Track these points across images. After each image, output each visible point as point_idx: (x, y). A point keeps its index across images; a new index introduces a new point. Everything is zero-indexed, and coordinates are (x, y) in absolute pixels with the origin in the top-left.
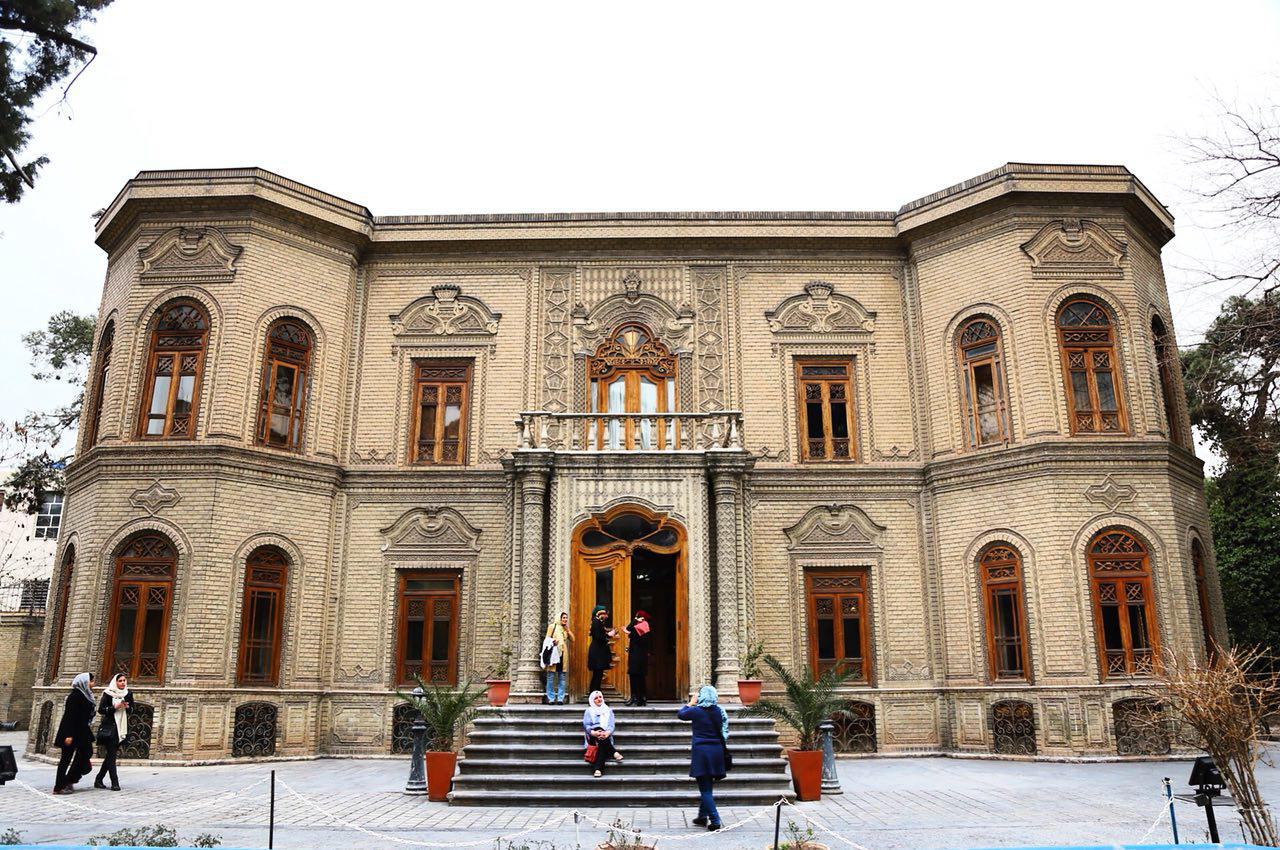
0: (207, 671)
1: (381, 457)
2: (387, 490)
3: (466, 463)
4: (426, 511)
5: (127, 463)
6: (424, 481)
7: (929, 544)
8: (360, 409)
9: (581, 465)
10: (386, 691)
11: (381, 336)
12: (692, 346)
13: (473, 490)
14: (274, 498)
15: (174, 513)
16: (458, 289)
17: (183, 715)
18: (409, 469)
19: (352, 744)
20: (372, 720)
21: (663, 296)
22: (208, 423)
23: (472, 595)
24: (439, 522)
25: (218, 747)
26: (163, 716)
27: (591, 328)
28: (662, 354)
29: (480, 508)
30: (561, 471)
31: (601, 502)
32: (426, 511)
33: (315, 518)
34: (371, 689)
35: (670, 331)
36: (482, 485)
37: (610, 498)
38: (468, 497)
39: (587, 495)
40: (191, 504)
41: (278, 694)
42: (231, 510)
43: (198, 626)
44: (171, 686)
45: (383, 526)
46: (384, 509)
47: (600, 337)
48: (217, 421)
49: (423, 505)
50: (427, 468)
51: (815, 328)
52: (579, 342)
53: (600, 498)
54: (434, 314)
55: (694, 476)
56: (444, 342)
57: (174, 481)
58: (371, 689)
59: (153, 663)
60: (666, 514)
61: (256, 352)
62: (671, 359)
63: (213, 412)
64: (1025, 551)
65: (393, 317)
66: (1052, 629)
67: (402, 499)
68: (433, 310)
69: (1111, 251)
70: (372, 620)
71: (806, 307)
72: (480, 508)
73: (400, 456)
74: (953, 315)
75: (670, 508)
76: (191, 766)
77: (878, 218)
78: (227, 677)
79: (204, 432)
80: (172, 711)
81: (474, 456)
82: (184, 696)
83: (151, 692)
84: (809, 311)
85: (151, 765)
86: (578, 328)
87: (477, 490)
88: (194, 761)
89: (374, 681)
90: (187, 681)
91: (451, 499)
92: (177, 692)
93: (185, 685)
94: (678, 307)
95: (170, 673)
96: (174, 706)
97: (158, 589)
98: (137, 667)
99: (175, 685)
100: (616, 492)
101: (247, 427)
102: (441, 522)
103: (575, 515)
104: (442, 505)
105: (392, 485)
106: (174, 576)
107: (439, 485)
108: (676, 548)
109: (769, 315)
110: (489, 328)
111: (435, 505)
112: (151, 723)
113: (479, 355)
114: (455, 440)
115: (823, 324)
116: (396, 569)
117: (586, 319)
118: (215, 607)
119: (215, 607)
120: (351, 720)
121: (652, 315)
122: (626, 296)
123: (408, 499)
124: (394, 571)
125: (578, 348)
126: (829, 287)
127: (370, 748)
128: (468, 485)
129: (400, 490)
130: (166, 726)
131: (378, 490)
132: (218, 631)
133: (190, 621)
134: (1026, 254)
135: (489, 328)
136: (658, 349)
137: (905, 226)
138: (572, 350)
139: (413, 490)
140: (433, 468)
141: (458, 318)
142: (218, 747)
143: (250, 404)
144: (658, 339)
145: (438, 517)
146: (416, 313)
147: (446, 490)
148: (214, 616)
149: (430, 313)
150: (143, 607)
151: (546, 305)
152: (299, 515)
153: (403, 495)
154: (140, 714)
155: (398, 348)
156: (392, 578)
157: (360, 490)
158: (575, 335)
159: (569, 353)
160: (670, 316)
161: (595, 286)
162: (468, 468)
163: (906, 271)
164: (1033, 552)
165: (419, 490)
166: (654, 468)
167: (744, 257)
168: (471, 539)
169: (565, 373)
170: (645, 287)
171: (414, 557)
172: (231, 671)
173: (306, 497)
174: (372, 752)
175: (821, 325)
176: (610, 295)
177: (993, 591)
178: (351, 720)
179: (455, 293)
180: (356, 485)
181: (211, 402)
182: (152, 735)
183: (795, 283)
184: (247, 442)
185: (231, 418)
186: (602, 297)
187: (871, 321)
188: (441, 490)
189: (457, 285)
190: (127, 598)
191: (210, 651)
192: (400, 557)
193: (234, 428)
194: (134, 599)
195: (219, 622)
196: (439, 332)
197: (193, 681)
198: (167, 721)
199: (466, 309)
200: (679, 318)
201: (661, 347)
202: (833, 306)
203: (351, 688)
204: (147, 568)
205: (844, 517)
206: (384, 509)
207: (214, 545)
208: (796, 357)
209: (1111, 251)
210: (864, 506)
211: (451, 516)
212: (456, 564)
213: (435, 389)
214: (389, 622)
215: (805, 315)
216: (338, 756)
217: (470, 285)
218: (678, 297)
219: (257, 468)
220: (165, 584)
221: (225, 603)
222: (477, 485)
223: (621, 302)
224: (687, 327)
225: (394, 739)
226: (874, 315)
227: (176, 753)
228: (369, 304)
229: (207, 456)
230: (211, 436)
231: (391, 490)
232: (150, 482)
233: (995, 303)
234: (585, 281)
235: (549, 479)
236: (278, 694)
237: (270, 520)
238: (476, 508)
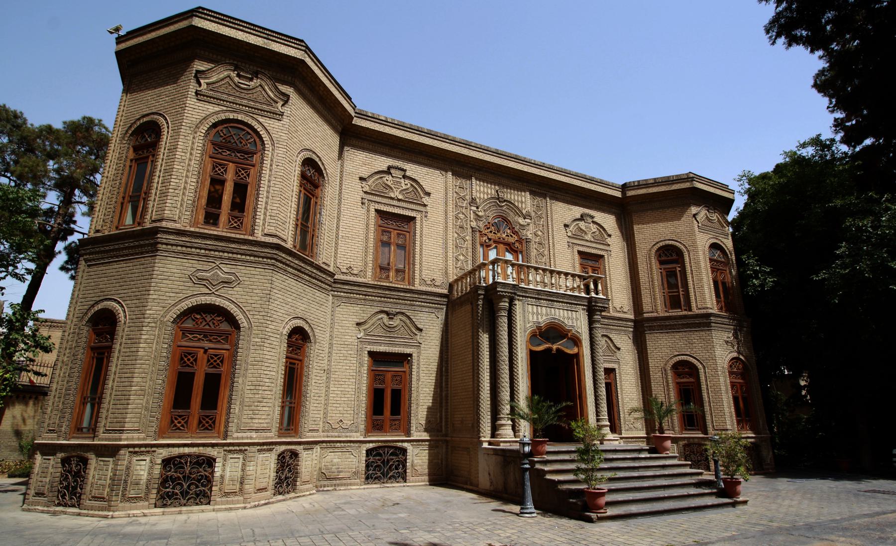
0: (262, 425)
1: (355, 272)
2: (361, 296)
3: (411, 281)
4: (387, 313)
5: (188, 244)
6: (387, 292)
8: (340, 237)
9: (530, 295)
10: (362, 439)
11: (354, 192)
12: (531, 235)
13: (417, 303)
14: (302, 291)
15: (236, 293)
16: (405, 171)
17: (244, 464)
18: (376, 283)
19: (335, 479)
20: (350, 460)
21: (516, 204)
22: (264, 224)
23: (418, 372)
24: (396, 322)
25: (264, 489)
26: (224, 465)
27: (480, 214)
28: (516, 237)
29: (421, 315)
30: (518, 298)
31: (540, 320)
32: (387, 313)
33: (321, 309)
34: (350, 437)
35: (520, 225)
36: (423, 300)
37: (544, 318)
38: (413, 307)
39: (533, 314)
40: (250, 287)
41: (299, 443)
42: (280, 296)
43: (257, 387)
44: (233, 438)
45: (358, 321)
46: (358, 309)
47: (485, 220)
48: (271, 224)
49: (385, 309)
50: (388, 285)
51: (586, 238)
52: (474, 221)
53: (539, 317)
54: (389, 183)
55: (583, 309)
56: (395, 203)
57: (234, 267)
58: (350, 437)
59: (211, 419)
60: (571, 330)
61: (296, 179)
62: (520, 241)
63: (268, 217)
64: (700, 366)
65: (361, 179)
66: (716, 407)
67: (371, 303)
68: (388, 179)
69: (725, 225)
70: (350, 387)
71: (582, 224)
72: (421, 315)
73: (369, 274)
74: (654, 243)
75: (573, 327)
76: (251, 508)
78: (273, 430)
79: (260, 231)
80: (232, 460)
81: (417, 281)
82: (246, 448)
83: (213, 445)
84: (583, 228)
85: (214, 510)
86: (474, 212)
87: (420, 303)
88: (253, 504)
89: (352, 431)
90: (248, 434)
91: (403, 307)
92: (239, 445)
93: (247, 438)
94: (524, 212)
95: (232, 427)
96: (235, 456)
97: (216, 355)
98: (195, 422)
99: (237, 438)
100: (547, 315)
101: (290, 234)
102: (398, 322)
103: (528, 325)
104: (398, 310)
105: (365, 293)
106: (236, 346)
107: (396, 297)
108: (576, 350)
109: (566, 226)
110: (424, 200)
111: (393, 310)
112: (213, 472)
113: (418, 216)
114: (406, 271)
115: (589, 236)
116: (368, 351)
117: (477, 208)
118: (268, 373)
119: (268, 373)
120: (335, 460)
121: (511, 213)
122: (498, 199)
123: (375, 304)
124: (366, 352)
125: (474, 224)
126: (592, 217)
127: (349, 481)
128: (415, 299)
129: (370, 297)
130: (228, 474)
131: (355, 295)
132: (269, 393)
133: (250, 383)
134: (696, 219)
135: (424, 200)
136: (514, 234)
138: (470, 225)
139: (379, 298)
140: (391, 285)
141: (405, 190)
142: (264, 489)
143: (292, 217)
144: (514, 228)
145: (396, 318)
146: (377, 179)
147: (400, 301)
148: (267, 380)
149: (386, 182)
150: (201, 371)
151: (455, 195)
152: (314, 306)
153: (373, 300)
154: (200, 465)
155: (366, 200)
156: (366, 358)
157: (342, 294)
158: (472, 216)
159: (469, 227)
160: (520, 216)
161: (482, 190)
162: (413, 288)
163: (622, 216)
164: (704, 367)
165: (383, 299)
166: (565, 303)
167: (555, 192)
168: (416, 335)
169: (467, 238)
170: (507, 197)
171: (380, 344)
172: (276, 425)
173: (318, 293)
174: (351, 484)
175: (589, 237)
176: (489, 196)
177: (680, 386)
178: (335, 460)
179: (403, 173)
180: (340, 290)
181: (266, 208)
182: (214, 483)
183: (577, 211)
184: (289, 245)
185: (281, 224)
186: (486, 197)
187: (609, 239)
188: (398, 301)
189: (405, 168)
190: (185, 362)
191: (264, 409)
192: (370, 343)
193: (283, 232)
194: (192, 363)
195: (270, 384)
196: (393, 196)
197: (254, 435)
198: (228, 469)
199: (409, 185)
200: (524, 218)
201: (516, 233)
202: (594, 228)
203: (336, 437)
204: (205, 336)
206: (358, 309)
207: (269, 323)
208: (580, 252)
209: (725, 225)
211: (404, 318)
212: (407, 351)
213: (390, 232)
214: (364, 388)
215: (581, 229)
216: (325, 489)
217: (413, 170)
218: (524, 206)
219: (295, 266)
220: (224, 351)
221: (275, 370)
222: (419, 300)
223: (495, 202)
224: (528, 225)
225: (366, 473)
226: (610, 236)
227: (236, 498)
228: (345, 166)
229: (266, 250)
230: (266, 235)
231: (364, 297)
232: (210, 264)
233: (679, 240)
234: (477, 185)
236: (299, 443)
237: (301, 308)
238: (419, 315)
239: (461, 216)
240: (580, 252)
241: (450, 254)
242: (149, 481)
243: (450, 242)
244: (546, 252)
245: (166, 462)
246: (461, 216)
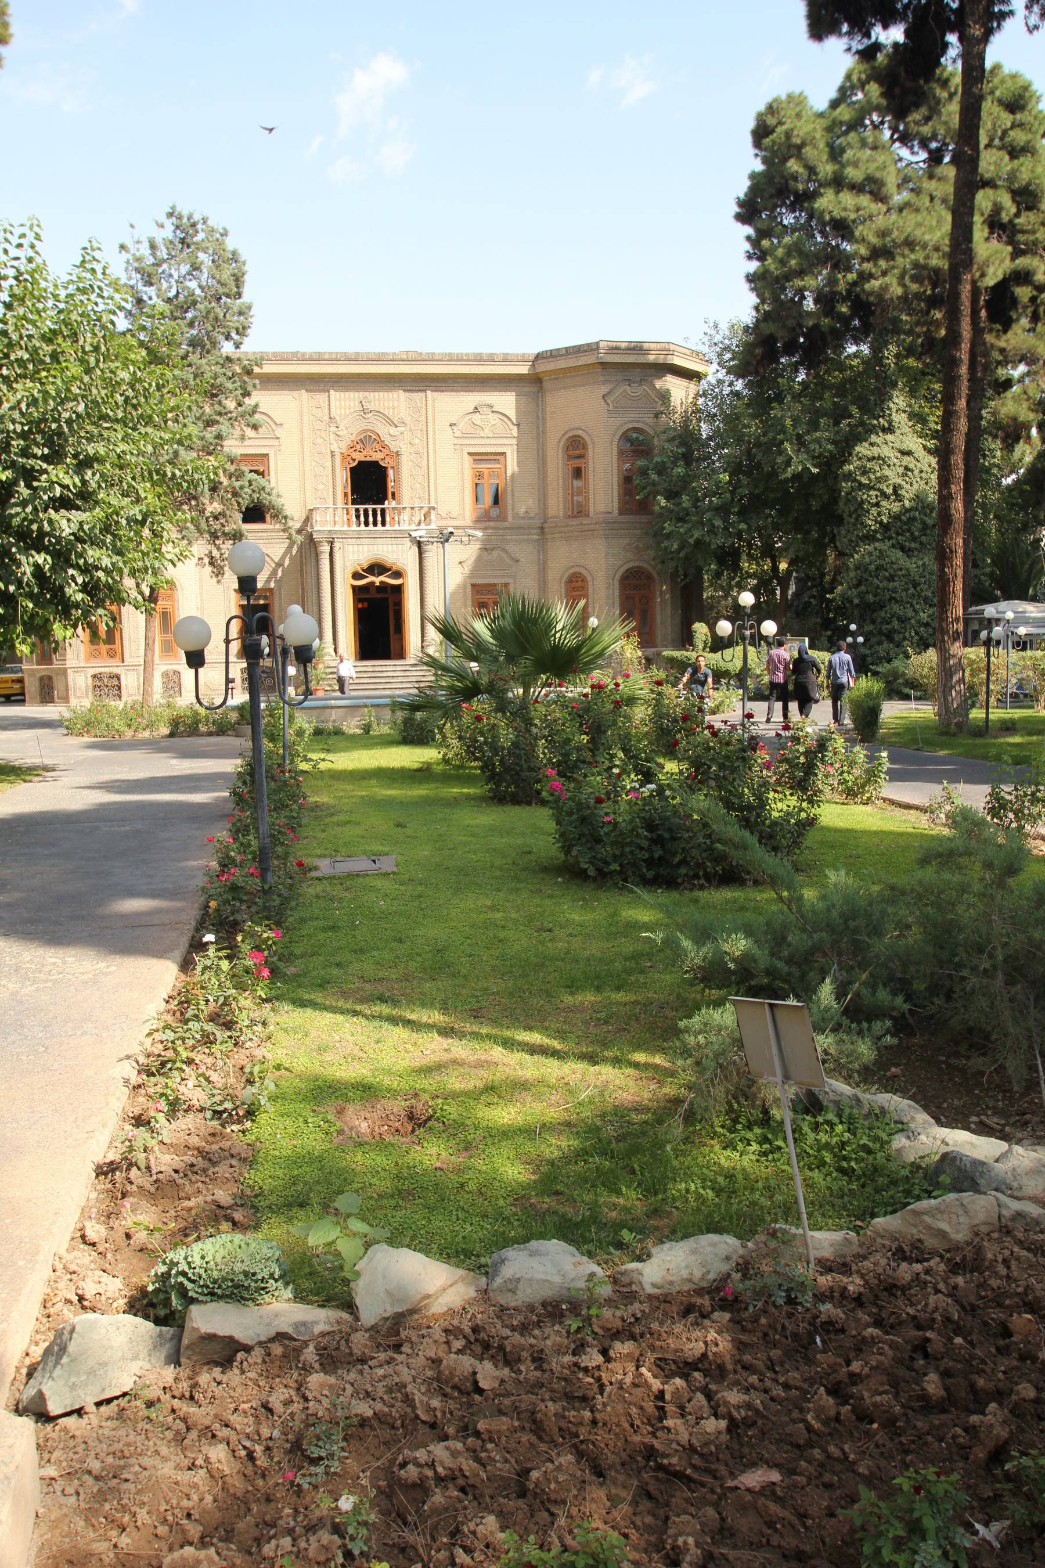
7: (543, 568)
64: (589, 579)
71: (476, 418)
77: (523, 359)
84: (478, 422)
125: (335, 447)
137: (541, 368)
202: (494, 419)
205: (495, 553)
208: (470, 454)
210: (507, 547)
235: (331, 543)
239: (320, 441)
240: (470, 454)
241: (308, 486)
242: (87, 686)
243: (307, 473)
244: (425, 462)
245: (94, 676)
246: (320, 441)
